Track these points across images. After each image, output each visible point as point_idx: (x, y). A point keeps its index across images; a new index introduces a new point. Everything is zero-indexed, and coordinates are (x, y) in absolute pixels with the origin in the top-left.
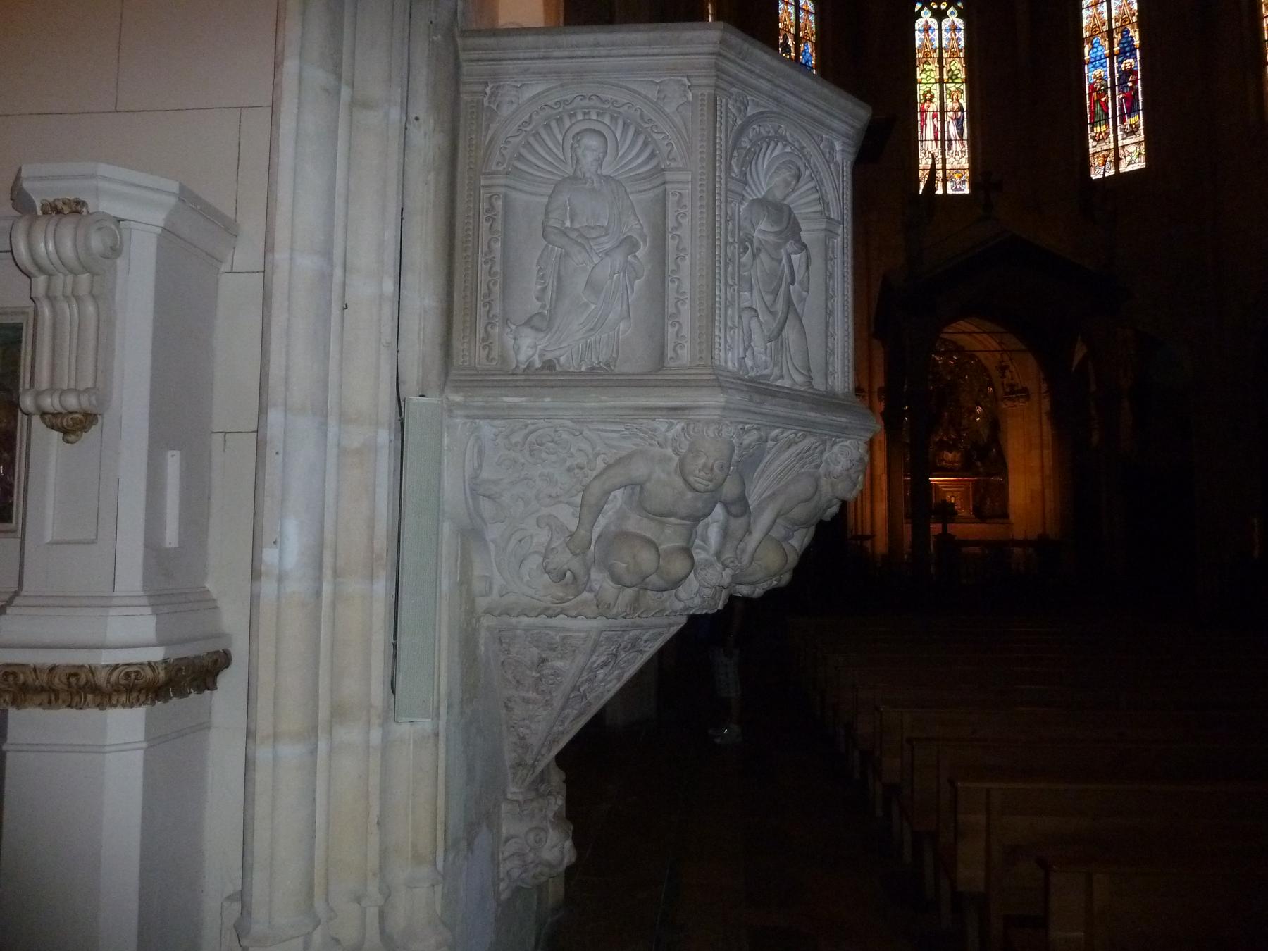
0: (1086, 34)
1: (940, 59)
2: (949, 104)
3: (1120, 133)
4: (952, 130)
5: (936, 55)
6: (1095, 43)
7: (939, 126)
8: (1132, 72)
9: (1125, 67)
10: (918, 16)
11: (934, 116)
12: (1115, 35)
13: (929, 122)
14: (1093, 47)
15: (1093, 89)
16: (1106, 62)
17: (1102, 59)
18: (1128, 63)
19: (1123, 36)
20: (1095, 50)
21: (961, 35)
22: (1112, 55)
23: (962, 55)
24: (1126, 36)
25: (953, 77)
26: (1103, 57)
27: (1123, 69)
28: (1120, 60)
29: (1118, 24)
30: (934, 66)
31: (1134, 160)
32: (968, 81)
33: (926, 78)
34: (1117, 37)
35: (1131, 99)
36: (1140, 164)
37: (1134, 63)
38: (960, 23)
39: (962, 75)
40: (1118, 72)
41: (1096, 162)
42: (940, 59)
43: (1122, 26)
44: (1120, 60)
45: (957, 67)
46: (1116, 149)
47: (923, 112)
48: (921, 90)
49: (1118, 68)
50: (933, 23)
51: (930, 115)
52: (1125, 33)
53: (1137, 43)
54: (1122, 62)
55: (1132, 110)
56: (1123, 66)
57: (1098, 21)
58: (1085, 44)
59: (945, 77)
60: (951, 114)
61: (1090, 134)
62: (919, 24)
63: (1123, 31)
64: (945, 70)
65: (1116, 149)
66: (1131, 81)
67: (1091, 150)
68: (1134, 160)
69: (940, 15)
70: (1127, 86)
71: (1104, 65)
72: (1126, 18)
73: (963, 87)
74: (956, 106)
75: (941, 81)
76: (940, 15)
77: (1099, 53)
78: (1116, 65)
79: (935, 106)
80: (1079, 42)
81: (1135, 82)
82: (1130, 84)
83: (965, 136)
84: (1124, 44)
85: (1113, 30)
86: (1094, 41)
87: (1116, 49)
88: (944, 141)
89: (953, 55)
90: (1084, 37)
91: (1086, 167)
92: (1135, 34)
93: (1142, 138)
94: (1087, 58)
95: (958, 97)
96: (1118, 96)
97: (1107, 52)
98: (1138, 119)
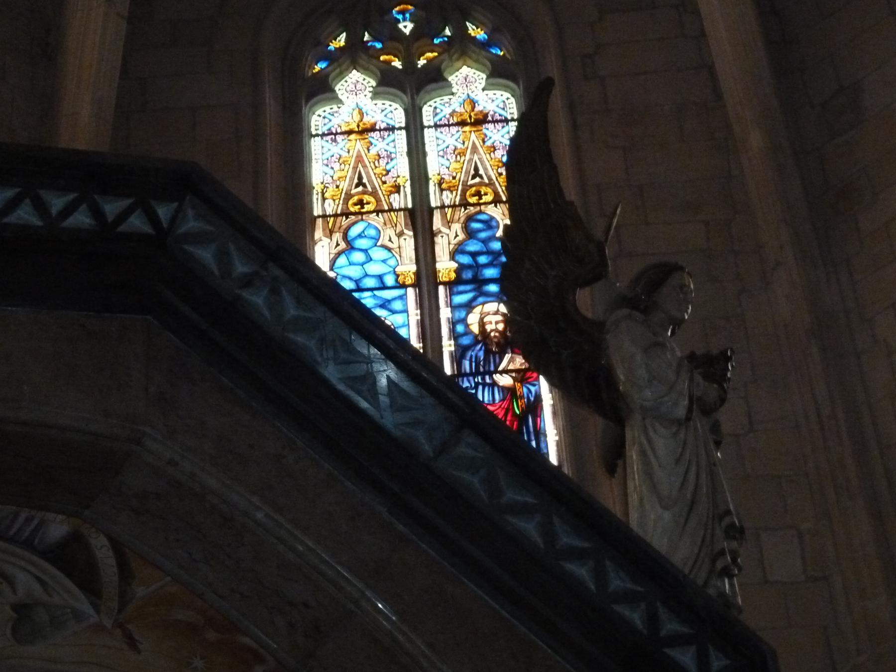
6: (360, 236)
9: (482, 324)
12: (437, 222)
14: (350, 247)
16: (402, 297)
17: (384, 287)
19: (471, 234)
20: (358, 257)
24: (483, 235)
26: (390, 280)
27: (475, 329)
28: (459, 299)
29: (448, 198)
40: (455, 336)
43: (465, 204)
44: (459, 299)
49: (453, 323)
54: (469, 307)
56: (473, 320)
57: (371, 177)
58: (318, 234)
63: (470, 219)
66: (506, 371)
70: (494, 384)
71: (397, 305)
72: (481, 184)
77: (374, 268)
78: (445, 313)
82: (505, 380)
84: (474, 255)
85: (431, 211)
86: (354, 232)
87: (445, 267)
90: (317, 211)
97: (409, 268)
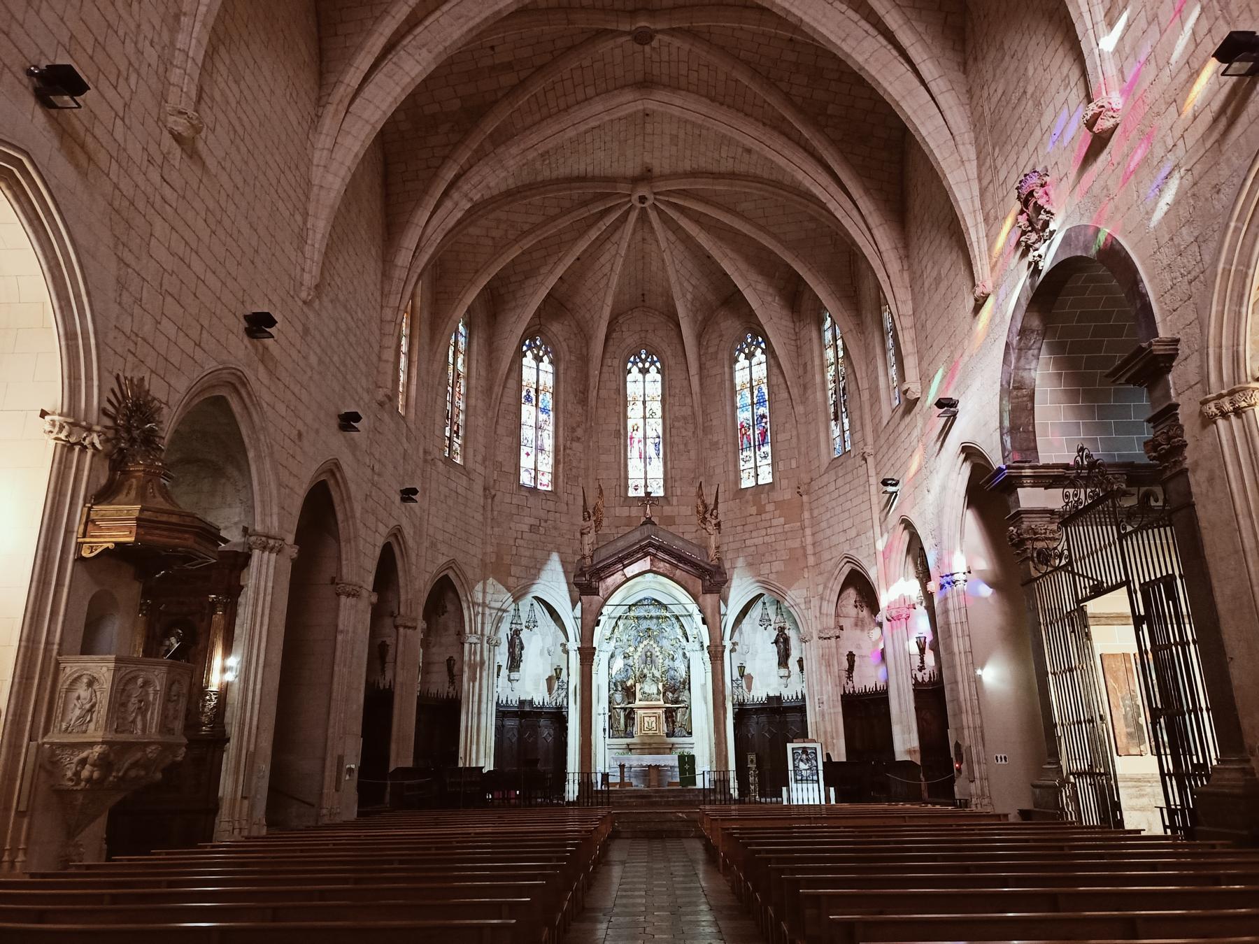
0: (738, 388)
1: (644, 402)
2: (650, 433)
3: (758, 457)
4: (651, 451)
5: (642, 399)
7: (642, 448)
8: (763, 416)
10: (630, 372)
11: (639, 441)
13: (636, 444)
15: (742, 427)
18: (764, 410)
21: (659, 385)
22: (753, 403)
23: (660, 398)
25: (653, 414)
30: (640, 404)
31: (766, 477)
32: (663, 417)
33: (634, 414)
34: (756, 392)
35: (764, 434)
36: (770, 480)
37: (764, 410)
38: (659, 377)
39: (659, 413)
41: (744, 475)
42: (644, 402)
45: (656, 407)
46: (756, 467)
47: (631, 438)
48: (630, 423)
50: (640, 376)
51: (636, 440)
52: (760, 390)
53: (767, 397)
55: (763, 443)
59: (647, 415)
60: (652, 440)
61: (741, 457)
62: (630, 378)
64: (647, 410)
65: (756, 467)
67: (742, 468)
68: (766, 477)
69: (644, 371)
73: (660, 421)
74: (654, 435)
75: (645, 418)
76: (644, 371)
79: (639, 435)
80: (733, 392)
81: (766, 423)
83: (661, 456)
87: (755, 400)
88: (645, 458)
89: (653, 399)
91: (738, 479)
92: (765, 390)
93: (770, 461)
94: (738, 405)
95: (656, 426)
96: (757, 432)
98: (767, 449)
